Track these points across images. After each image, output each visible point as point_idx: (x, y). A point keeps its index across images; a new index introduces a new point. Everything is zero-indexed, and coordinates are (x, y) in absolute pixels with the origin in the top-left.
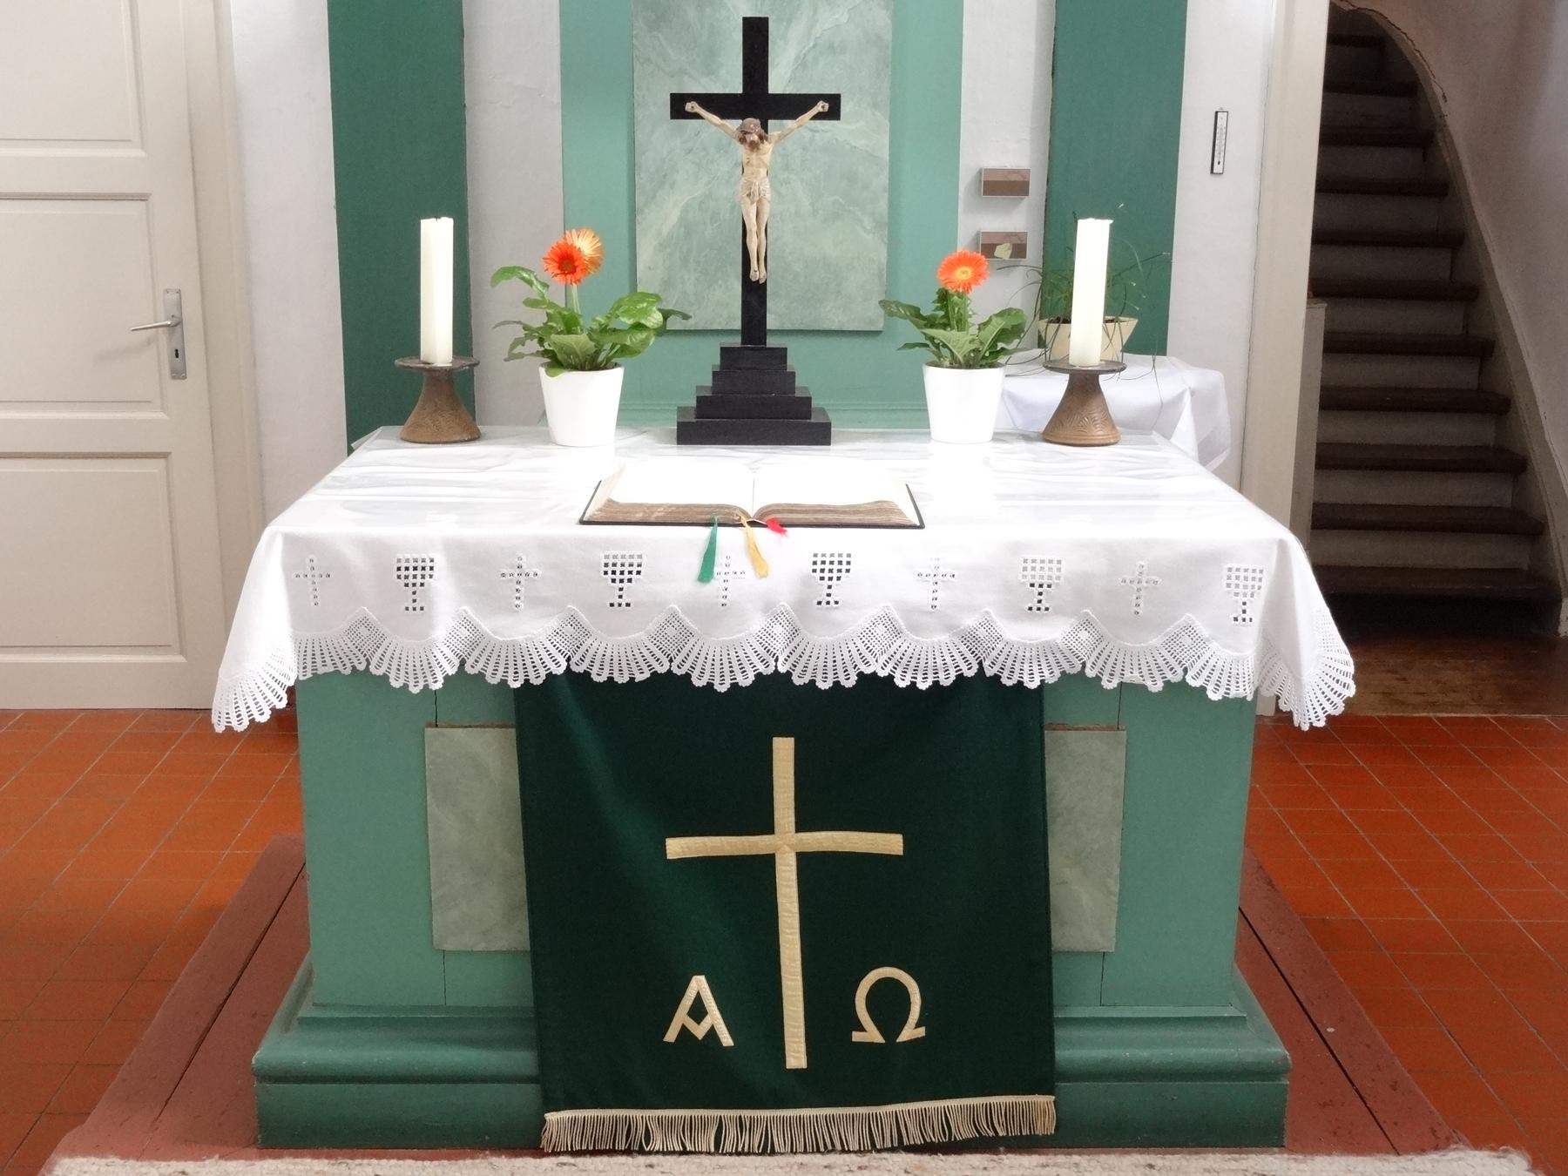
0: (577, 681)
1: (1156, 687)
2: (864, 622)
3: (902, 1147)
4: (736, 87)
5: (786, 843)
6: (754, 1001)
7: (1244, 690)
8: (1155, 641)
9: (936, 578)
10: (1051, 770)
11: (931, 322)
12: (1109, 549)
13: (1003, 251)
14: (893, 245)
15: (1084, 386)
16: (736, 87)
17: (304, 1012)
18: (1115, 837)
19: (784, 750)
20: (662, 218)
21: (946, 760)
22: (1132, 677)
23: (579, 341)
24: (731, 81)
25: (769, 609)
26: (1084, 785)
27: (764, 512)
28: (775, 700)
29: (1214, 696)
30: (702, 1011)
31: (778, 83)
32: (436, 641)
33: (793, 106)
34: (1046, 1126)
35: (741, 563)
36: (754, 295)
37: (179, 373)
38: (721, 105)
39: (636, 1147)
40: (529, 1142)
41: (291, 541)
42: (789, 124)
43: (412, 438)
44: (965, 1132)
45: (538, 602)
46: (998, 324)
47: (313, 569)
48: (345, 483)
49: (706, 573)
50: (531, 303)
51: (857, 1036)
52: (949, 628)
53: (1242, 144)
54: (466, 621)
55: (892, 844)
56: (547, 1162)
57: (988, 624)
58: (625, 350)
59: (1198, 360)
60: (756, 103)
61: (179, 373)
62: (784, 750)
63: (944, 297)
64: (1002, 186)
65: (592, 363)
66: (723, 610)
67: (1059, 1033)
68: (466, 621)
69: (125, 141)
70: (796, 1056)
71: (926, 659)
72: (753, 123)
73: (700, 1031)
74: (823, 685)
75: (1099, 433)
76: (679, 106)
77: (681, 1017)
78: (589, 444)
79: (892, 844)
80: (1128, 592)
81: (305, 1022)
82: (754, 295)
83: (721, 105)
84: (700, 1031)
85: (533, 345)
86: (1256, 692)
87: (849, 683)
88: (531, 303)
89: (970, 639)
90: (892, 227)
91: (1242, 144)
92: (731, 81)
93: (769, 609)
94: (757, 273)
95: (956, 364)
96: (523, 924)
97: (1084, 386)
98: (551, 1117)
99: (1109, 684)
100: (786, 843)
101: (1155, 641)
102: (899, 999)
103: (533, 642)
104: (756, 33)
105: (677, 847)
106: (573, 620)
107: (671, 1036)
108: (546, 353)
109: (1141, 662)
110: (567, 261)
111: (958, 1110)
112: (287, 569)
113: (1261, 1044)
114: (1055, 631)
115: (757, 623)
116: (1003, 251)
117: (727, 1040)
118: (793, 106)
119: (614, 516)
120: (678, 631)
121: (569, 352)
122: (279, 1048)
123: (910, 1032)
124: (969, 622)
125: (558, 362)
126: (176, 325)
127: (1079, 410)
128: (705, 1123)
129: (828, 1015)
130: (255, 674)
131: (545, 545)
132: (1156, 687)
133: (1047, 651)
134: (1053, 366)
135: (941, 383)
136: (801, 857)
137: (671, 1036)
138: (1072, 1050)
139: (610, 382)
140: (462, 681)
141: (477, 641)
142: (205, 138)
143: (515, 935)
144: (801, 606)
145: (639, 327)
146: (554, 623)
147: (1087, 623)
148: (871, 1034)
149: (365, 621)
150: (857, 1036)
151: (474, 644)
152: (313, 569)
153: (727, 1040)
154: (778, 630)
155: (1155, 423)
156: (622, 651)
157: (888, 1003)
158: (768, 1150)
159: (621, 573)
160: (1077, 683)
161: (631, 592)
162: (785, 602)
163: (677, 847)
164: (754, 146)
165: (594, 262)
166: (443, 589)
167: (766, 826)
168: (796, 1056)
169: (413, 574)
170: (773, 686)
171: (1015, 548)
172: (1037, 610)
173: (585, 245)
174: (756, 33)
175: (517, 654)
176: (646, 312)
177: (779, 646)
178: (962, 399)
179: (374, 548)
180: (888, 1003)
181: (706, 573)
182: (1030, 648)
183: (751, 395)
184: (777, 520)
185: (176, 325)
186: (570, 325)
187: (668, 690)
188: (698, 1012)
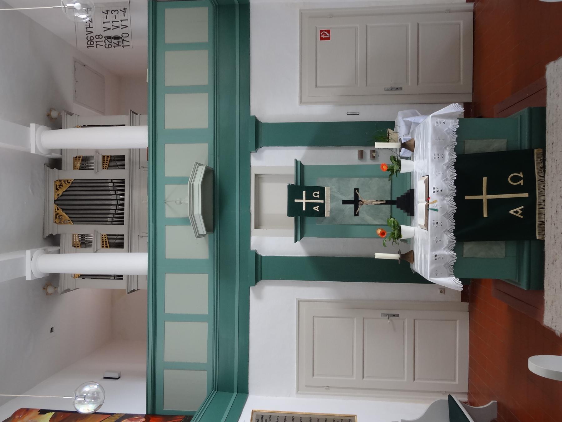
0: (455, 232)
1: (457, 136)
2: (445, 185)
3: (544, 176)
4: (353, 206)
5: (485, 197)
6: (515, 203)
7: (457, 121)
8: (448, 136)
9: (437, 173)
10: (471, 152)
11: (393, 172)
12: (433, 145)
13: (374, 154)
14: (375, 177)
15: (404, 145)
16: (353, 206)
17: (517, 281)
18: (485, 140)
19: (467, 197)
20: (369, 219)
21: (469, 171)
22: (455, 140)
23: (396, 232)
24: (353, 206)
25: (443, 200)
26: (474, 146)
27: (426, 201)
28: (458, 199)
29: (458, 126)
30: (517, 211)
31: (351, 197)
32: (448, 254)
33: (356, 196)
34: (541, 150)
35: (435, 204)
36: (387, 203)
37: (397, 315)
38: (356, 208)
39: (543, 224)
40: (542, 242)
41: (430, 277)
42: (359, 196)
43: (413, 262)
44: (542, 165)
45: (441, 237)
46: (393, 161)
47: (435, 273)
48: (421, 270)
49: (436, 210)
50: (390, 240)
51: (522, 184)
52: (446, 170)
53: (353, 109)
54: (444, 249)
55: (485, 179)
56: (545, 239)
57: (445, 164)
58: (398, 225)
59: (396, 116)
60: (356, 202)
61: (397, 315)
62: (467, 197)
63: (388, 170)
64: (362, 155)
65: (400, 230)
66: (443, 208)
67: (523, 149)
68: (444, 249)
69: (353, 321)
70: (526, 195)
71: (452, 174)
72: (359, 203)
73: (520, 212)
74: (456, 191)
75: (412, 142)
76: (356, 215)
77: (518, 215)
78: (415, 230)
79: (485, 179)
80: (439, 141)
81: (519, 280)
82: (387, 203)
83: (356, 208)
84: (520, 212)
85: (396, 240)
86: (458, 119)
87: (455, 187)
88: (390, 240)
89: (448, 167)
90: (371, 177)
91: (353, 109)
92: (353, 206)
93: (443, 200)
94: (384, 202)
95: (400, 168)
96: (500, 242)
97: (404, 145)
98: (537, 238)
99: (456, 144)
100: (485, 197)
101: (448, 136)
102: (516, 177)
103: (448, 238)
104: (345, 202)
105: (485, 215)
106: (444, 232)
107: (522, 217)
108: (398, 239)
109: (452, 139)
110: (383, 234)
111: (537, 167)
112: (435, 278)
113: (525, 112)
114: (447, 153)
115: (445, 202)
116: (374, 154)
117: (522, 207)
118: (356, 196)
119: (427, 225)
120: (446, 215)
121: (397, 235)
122: (524, 286)
123: (521, 175)
124: (445, 167)
125: (400, 235)
126: (389, 315)
127: (408, 146)
128: (539, 211)
129: (518, 189)
130: (453, 283)
131: (431, 236)
132: (457, 136)
133: (450, 154)
134: (400, 151)
135: (403, 170)
136: (487, 195)
137: (522, 217)
138: (526, 145)
139: (403, 227)
140: (455, 250)
141: (448, 247)
142: (353, 306)
143: (502, 244)
144: (442, 195)
145: (394, 222)
146: (445, 235)
147: (445, 148)
148: (521, 182)
149: (445, 265)
150: (522, 184)
151: (448, 248)
152: (435, 273)
153: (522, 207)
154: (446, 198)
155: (409, 125)
156: (450, 224)
157: (515, 179)
158: (544, 200)
159: (436, 224)
160: (456, 149)
161: (439, 222)
162: (441, 198)
163: (485, 215)
164: (363, 203)
165: (382, 230)
166: (438, 252)
167: (482, 200)
168: (526, 195)
169: (436, 258)
170: (455, 199)
171: (432, 160)
172: (443, 156)
173: (379, 231)
174: (345, 202)
175: (450, 241)
176: (391, 221)
177: (449, 199)
178: (406, 166)
179: (432, 263)
180: (515, 179)
181: (436, 210)
182: (449, 157)
183: (406, 203)
184: (427, 199)
185: (389, 315)
186: (393, 234)
187: (456, 216)
188: (517, 212)
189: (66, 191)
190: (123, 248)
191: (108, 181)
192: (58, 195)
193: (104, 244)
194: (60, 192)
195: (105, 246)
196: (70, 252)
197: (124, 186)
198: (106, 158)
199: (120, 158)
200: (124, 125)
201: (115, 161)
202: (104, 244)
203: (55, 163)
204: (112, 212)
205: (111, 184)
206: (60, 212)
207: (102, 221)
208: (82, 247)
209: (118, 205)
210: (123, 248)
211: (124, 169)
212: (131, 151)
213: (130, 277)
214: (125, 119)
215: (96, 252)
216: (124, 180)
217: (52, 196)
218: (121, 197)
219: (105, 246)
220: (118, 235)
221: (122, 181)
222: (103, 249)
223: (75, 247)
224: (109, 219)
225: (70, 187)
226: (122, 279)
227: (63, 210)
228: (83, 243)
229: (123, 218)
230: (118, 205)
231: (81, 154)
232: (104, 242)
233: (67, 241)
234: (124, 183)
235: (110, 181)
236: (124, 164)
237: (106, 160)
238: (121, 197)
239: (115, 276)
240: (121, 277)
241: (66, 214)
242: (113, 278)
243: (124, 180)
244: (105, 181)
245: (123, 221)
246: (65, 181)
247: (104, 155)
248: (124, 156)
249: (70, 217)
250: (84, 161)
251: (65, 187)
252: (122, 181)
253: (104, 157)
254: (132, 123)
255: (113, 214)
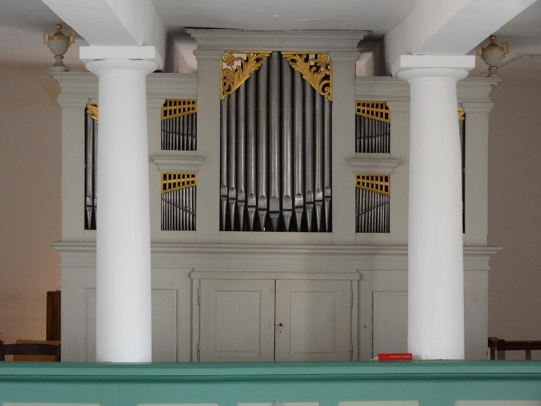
189: (304, 81)
190: (163, 228)
191: (328, 192)
192: (294, 61)
193: (172, 181)
194: (301, 67)
195: (168, 182)
196: (150, 95)
197: (314, 229)
198: (384, 183)
199: (382, 219)
200: (464, 232)
201: (376, 215)
202: (172, 181)
203: (375, 44)
204: (252, 201)
205: (319, 196)
206: (252, 67)
207: (225, 182)
208: (163, 123)
209: (269, 212)
210: (163, 228)
211: (357, 231)
212: (402, 248)
213: (91, 248)
214: (480, 234)
215: (151, 159)
216: (330, 230)
217: (290, 47)
218: (287, 221)
219: (168, 182)
220: (194, 215)
221: (326, 226)
222: (161, 177)
223: (165, 105)
224: (233, 194)
225: (314, 91)
226: (86, 227)
227: (257, 73)
228: (176, 128)
229: (237, 229)
230: (269, 212)
231: (393, 120)
232: (176, 181)
233: (178, 162)
234: (323, 230)
235: (328, 192)
236: (368, 230)
237: (379, 183)
238: (287, 221)
239: (94, 207)
240: (91, 224)
241: (247, 82)
242: (89, 201)
243: (330, 230)
244: (328, 183)
245: (228, 229)
246: (327, 77)
247: (392, 179)
248: (387, 230)
249: (238, 91)
250: (375, 131)
251: (314, 81)
252: (326, 226)
253: (387, 179)
254: (469, 250)
255: (246, 201)
